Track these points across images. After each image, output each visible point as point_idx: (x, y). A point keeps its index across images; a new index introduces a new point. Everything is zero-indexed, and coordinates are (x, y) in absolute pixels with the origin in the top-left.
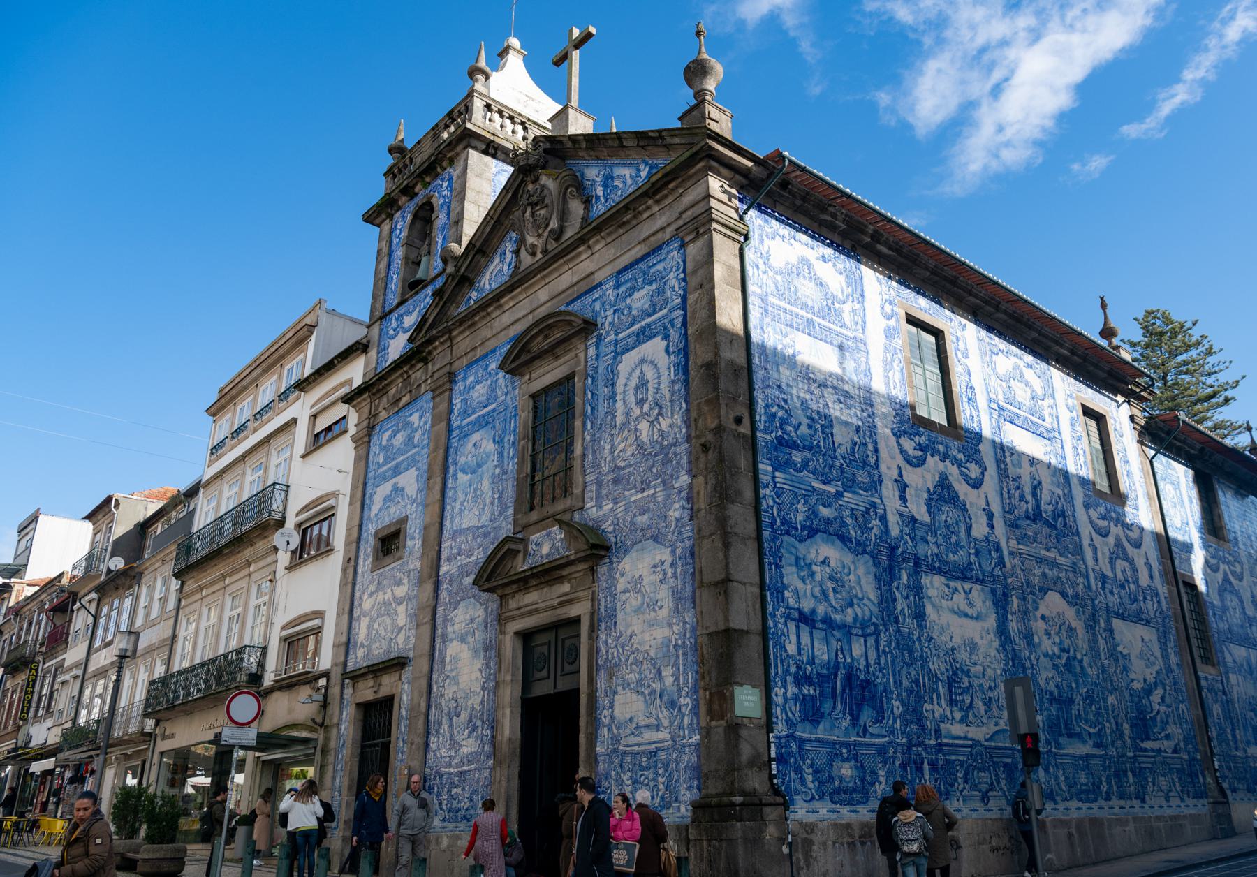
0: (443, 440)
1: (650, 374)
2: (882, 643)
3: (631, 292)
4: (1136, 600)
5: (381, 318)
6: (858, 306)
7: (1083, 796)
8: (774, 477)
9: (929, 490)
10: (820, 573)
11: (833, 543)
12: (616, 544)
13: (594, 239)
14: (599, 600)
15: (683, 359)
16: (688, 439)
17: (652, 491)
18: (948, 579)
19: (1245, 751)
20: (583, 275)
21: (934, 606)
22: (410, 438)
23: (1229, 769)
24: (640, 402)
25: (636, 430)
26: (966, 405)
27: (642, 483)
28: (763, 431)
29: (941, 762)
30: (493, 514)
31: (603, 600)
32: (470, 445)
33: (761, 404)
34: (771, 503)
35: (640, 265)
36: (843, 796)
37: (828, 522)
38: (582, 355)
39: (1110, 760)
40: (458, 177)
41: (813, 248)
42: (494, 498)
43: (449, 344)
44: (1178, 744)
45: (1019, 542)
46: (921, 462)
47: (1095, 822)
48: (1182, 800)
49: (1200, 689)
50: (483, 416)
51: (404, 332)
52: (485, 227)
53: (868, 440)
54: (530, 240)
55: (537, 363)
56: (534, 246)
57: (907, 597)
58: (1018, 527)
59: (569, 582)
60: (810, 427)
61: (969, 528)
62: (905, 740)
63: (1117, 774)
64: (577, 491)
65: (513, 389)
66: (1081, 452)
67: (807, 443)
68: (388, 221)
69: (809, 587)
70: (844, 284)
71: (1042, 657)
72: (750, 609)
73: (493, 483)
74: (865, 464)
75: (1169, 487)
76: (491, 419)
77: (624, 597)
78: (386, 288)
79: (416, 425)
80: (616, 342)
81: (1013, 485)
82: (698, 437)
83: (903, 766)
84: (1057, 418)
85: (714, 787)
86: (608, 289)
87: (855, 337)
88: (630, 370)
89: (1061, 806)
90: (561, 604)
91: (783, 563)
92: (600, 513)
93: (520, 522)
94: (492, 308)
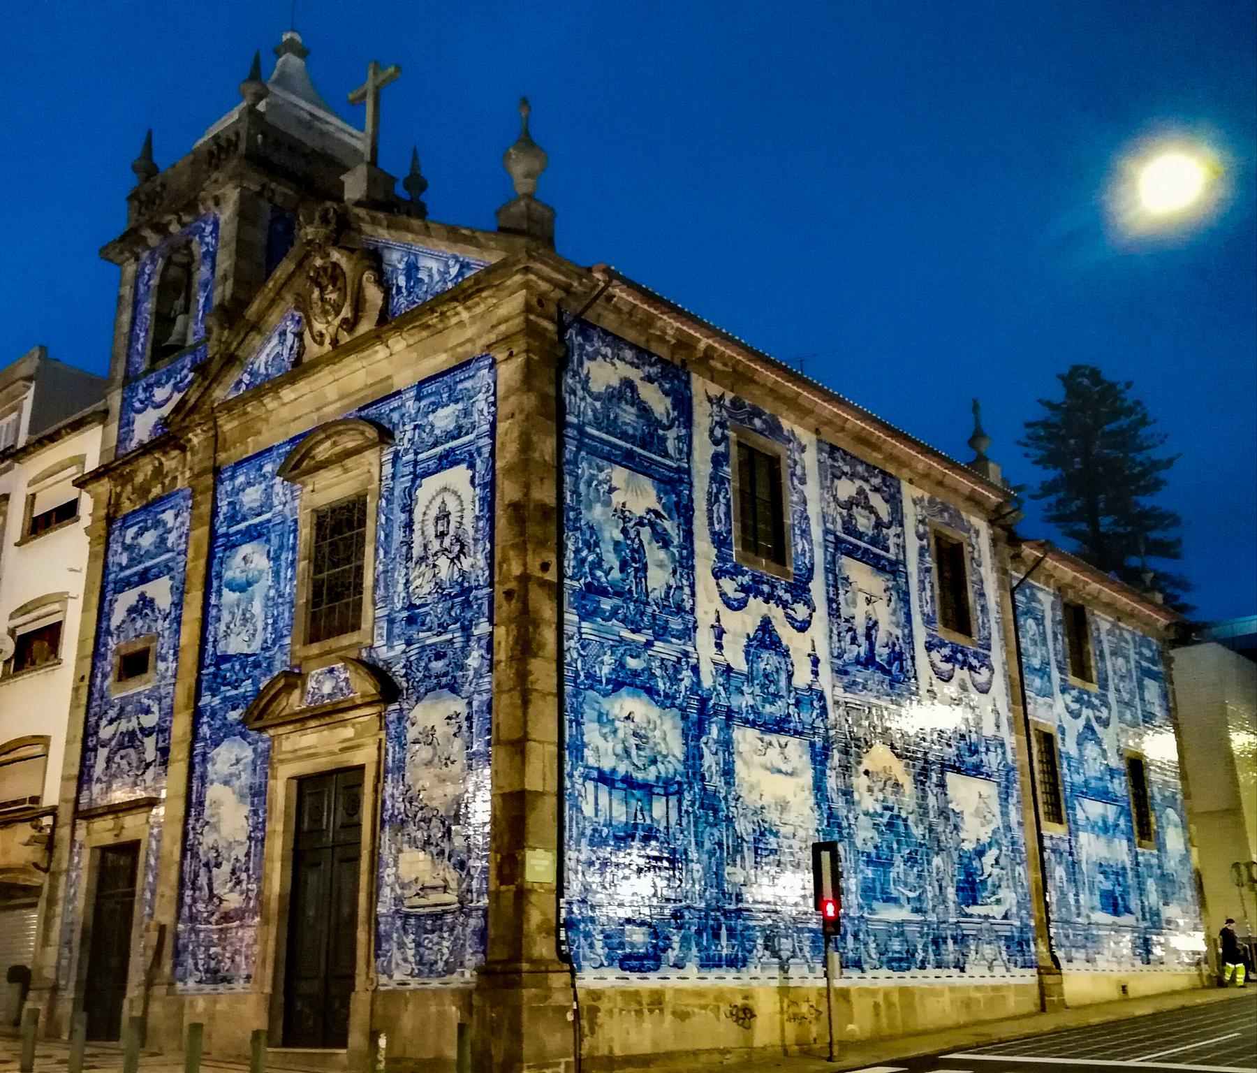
0: (205, 549)
1: (452, 506)
2: (685, 803)
3: (436, 406)
4: (976, 752)
6: (683, 432)
7: (894, 964)
8: (580, 628)
9: (748, 636)
10: (624, 729)
11: (639, 696)
12: (407, 689)
14: (387, 750)
16: (491, 584)
17: (449, 636)
18: (762, 732)
19: (1088, 917)
21: (746, 763)
22: (162, 540)
23: (1067, 937)
24: (441, 535)
25: (435, 566)
26: (798, 539)
27: (440, 625)
28: (571, 578)
29: (739, 928)
30: (265, 641)
31: (391, 750)
32: (238, 559)
33: (571, 547)
34: (575, 656)
36: (633, 963)
37: (635, 674)
39: (929, 926)
40: (226, 223)
41: (637, 368)
42: (267, 624)
43: (212, 433)
44: (1010, 909)
45: (846, 689)
46: (740, 605)
47: (905, 992)
48: (1008, 970)
49: (1042, 849)
50: (256, 526)
51: (155, 408)
53: (685, 582)
54: (319, 326)
56: (322, 335)
57: (716, 754)
58: (846, 673)
59: (353, 726)
60: (622, 570)
61: (790, 676)
62: (703, 905)
63: (935, 942)
64: (366, 625)
65: (293, 499)
66: (928, 586)
67: (618, 589)
68: (132, 260)
69: (611, 745)
70: (670, 407)
71: (861, 817)
72: (547, 770)
73: (266, 606)
74: (680, 609)
75: (1030, 621)
79: (169, 525)
80: (416, 463)
81: (844, 626)
82: (500, 583)
83: (699, 933)
84: (904, 547)
85: (500, 953)
86: (408, 400)
87: (679, 467)
89: (870, 974)
90: (343, 750)
91: (585, 720)
92: (392, 654)
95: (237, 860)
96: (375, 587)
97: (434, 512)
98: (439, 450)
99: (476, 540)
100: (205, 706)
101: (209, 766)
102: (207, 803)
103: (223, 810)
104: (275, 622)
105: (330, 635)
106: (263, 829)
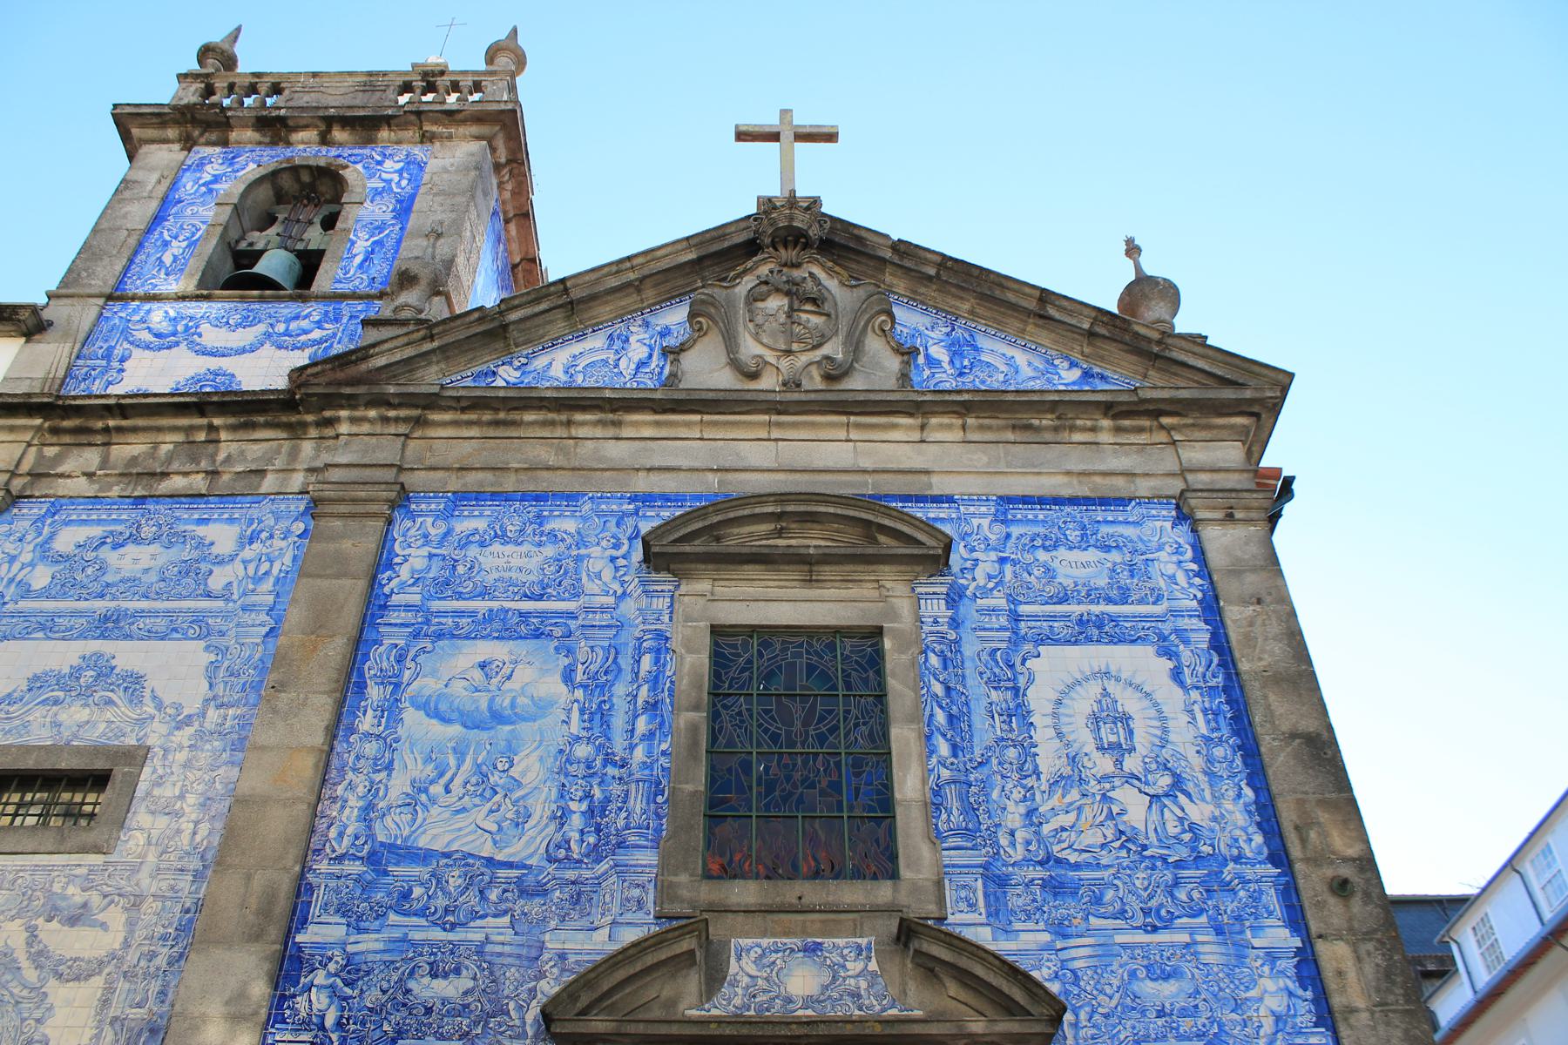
1: (1130, 703)
5: (110, 298)
13: (945, 420)
15: (1226, 707)
16: (1279, 856)
17: (1185, 938)
20: (890, 466)
24: (1117, 751)
25: (1105, 798)
35: (1068, 509)
38: (904, 606)
40: (446, 170)
50: (524, 614)
55: (751, 571)
76: (558, 632)
78: (136, 253)
88: (1069, 681)
93: (685, 893)
94: (588, 417)
96: (935, 804)
97: (1083, 703)
98: (1075, 609)
99: (1209, 774)
104: (590, 812)
105: (793, 874)
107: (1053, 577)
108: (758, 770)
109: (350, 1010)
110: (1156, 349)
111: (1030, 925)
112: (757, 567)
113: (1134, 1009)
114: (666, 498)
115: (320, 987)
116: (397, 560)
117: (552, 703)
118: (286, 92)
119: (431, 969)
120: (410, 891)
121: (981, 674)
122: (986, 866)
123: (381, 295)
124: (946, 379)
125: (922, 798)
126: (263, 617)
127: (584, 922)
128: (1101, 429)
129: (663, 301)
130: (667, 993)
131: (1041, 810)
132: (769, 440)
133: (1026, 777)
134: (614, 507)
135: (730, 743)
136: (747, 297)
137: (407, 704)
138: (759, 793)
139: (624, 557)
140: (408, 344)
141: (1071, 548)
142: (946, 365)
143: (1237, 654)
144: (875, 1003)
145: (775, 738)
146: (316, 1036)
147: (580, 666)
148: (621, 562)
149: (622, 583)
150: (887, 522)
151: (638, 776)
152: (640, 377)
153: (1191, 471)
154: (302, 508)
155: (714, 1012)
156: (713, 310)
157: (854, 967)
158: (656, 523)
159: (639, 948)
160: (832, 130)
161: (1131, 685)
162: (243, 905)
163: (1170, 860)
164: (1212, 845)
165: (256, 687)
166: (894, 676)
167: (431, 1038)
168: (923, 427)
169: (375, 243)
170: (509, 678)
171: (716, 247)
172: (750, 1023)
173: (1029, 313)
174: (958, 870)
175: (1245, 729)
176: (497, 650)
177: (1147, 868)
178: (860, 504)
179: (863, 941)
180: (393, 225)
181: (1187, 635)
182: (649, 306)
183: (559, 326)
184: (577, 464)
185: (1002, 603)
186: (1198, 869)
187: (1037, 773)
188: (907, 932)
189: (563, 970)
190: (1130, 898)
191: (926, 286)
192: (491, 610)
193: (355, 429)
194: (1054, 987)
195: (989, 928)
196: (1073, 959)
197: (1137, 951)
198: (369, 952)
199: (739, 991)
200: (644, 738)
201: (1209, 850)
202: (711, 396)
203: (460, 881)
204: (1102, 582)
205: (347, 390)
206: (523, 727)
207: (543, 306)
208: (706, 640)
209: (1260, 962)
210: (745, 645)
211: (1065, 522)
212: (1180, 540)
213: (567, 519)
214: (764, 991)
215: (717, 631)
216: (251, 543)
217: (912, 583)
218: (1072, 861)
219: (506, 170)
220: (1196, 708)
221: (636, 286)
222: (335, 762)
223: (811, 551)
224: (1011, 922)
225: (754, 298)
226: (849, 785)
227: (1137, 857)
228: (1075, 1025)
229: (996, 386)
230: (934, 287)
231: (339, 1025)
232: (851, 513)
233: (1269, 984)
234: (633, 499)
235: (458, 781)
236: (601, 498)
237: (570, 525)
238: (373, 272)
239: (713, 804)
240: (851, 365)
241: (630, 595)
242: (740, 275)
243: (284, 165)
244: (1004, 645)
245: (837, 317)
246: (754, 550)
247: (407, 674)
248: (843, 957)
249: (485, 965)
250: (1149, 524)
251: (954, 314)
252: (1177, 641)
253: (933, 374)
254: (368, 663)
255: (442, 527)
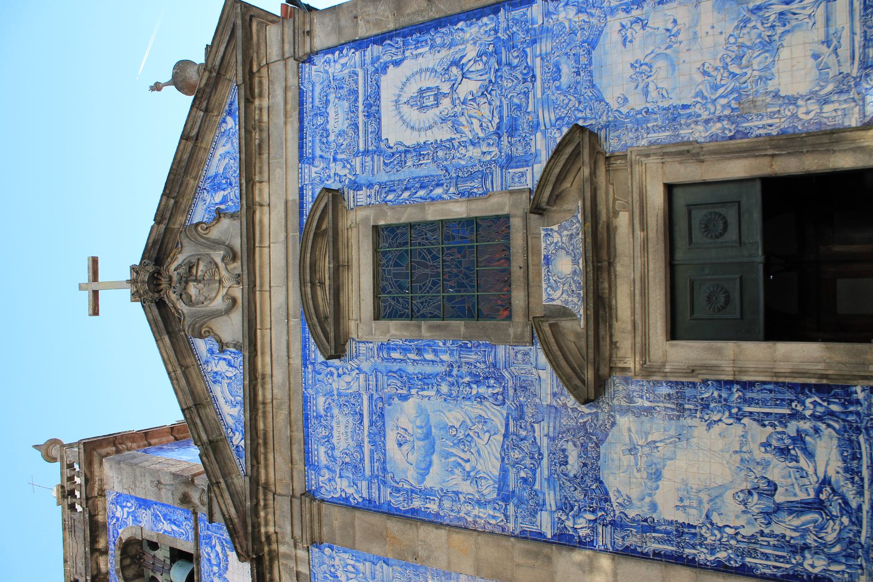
0: (376, 520)
1: (412, 89)
13: (257, 192)
15: (414, 37)
17: (538, 60)
24: (438, 96)
27: (525, 81)
31: (653, 136)
35: (306, 124)
38: (361, 214)
40: (121, 482)
50: (372, 423)
52: (178, 384)
55: (343, 300)
76: (380, 405)
77: (653, 94)
90: (644, 226)
93: (519, 330)
94: (260, 393)
95: (766, 445)
96: (467, 195)
97: (413, 114)
98: (361, 119)
99: (450, 46)
100: (553, 523)
101: (632, 513)
102: (681, 518)
103: (694, 483)
105: (508, 272)
106: (729, 383)
107: (344, 131)
108: (452, 292)
109: (585, 507)
110: (214, 74)
111: (533, 143)
112: (341, 296)
113: (576, 88)
114: (304, 347)
115: (574, 523)
116: (344, 495)
117: (419, 406)
118: (77, 577)
119: (563, 465)
120: (522, 478)
121: (397, 171)
122: (502, 167)
123: (195, 513)
124: (233, 193)
125: (466, 203)
126: (378, 567)
127: (536, 383)
128: (260, 105)
129: (193, 354)
130: (572, 338)
131: (471, 138)
132: (270, 291)
133: (453, 146)
134: (310, 376)
135: (438, 308)
136: (189, 306)
137: (422, 485)
138: (465, 291)
139: (338, 370)
140: (222, 496)
141: (328, 122)
142: (226, 193)
143: (385, 30)
144: (575, 226)
145: (435, 283)
146: (600, 524)
147: (398, 392)
148: (340, 371)
149: (352, 370)
150: (315, 224)
151: (457, 357)
152: (237, 364)
153: (283, 55)
154: (317, 550)
155: (582, 312)
156: (197, 325)
157: (556, 238)
158: (318, 353)
159: (549, 353)
160: (91, 261)
161: (402, 89)
162: (533, 567)
163: (497, 67)
164: (489, 45)
165: (416, 568)
166: (399, 219)
167: (599, 463)
168: (261, 205)
169: (165, 519)
170: (406, 430)
171: (161, 325)
172: (587, 293)
173: (195, 146)
174: (504, 182)
175: (426, 26)
176: (391, 438)
177: (501, 80)
178: (305, 239)
179: (543, 233)
180: (154, 509)
181: (374, 58)
182: (196, 361)
183: (209, 411)
184: (287, 398)
185: (358, 160)
186: (501, 53)
187: (451, 140)
188: (537, 209)
189: (562, 394)
190: (518, 89)
191: (181, 204)
192: (370, 442)
193: (271, 523)
194: (565, 130)
195: (535, 165)
196: (550, 120)
197: (546, 86)
198: (555, 499)
199: (570, 299)
200: (436, 355)
201: (491, 46)
202: (246, 325)
203: (516, 452)
204: (346, 104)
205: (250, 528)
206: (433, 421)
207: (198, 421)
208: (382, 322)
209: (550, 20)
210: (385, 301)
211: (313, 125)
212: (322, 61)
213: (318, 402)
214: (570, 286)
215: (377, 317)
216: (337, 577)
217: (348, 210)
218: (498, 120)
219: (120, 447)
220: (415, 53)
221: (185, 369)
222: (455, 523)
223: (332, 266)
224: (531, 154)
225: (190, 302)
226: (459, 243)
227: (496, 86)
228: (585, 119)
229: (237, 165)
230: (181, 200)
231: (593, 512)
232: (310, 244)
233: (562, 16)
234: (305, 365)
235: (463, 455)
236: (305, 383)
237: (321, 400)
238: (182, 519)
239: (471, 316)
240: (227, 246)
241: (359, 365)
242: (177, 310)
243: (121, 574)
244: (382, 159)
245: (200, 255)
246: (332, 298)
247: (406, 486)
248: (551, 243)
249: (560, 436)
250: (314, 78)
251: (196, 189)
252: (378, 63)
253: (231, 200)
254: (401, 508)
255: (325, 471)
